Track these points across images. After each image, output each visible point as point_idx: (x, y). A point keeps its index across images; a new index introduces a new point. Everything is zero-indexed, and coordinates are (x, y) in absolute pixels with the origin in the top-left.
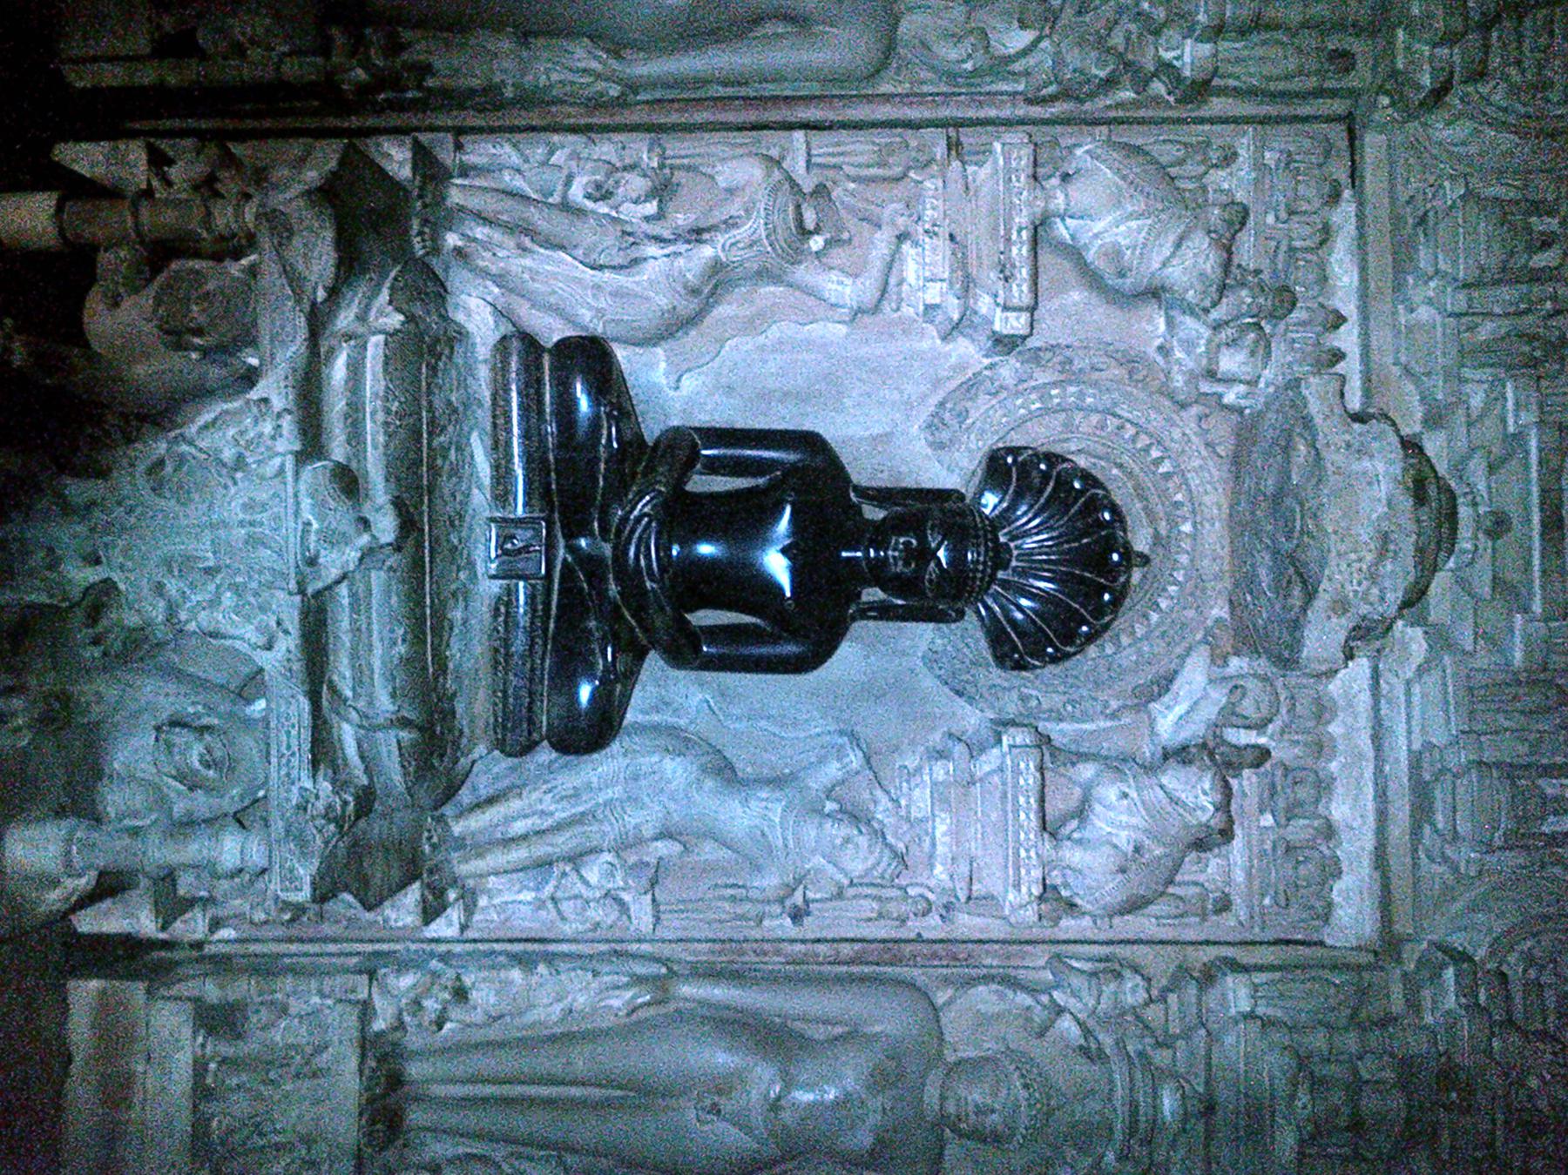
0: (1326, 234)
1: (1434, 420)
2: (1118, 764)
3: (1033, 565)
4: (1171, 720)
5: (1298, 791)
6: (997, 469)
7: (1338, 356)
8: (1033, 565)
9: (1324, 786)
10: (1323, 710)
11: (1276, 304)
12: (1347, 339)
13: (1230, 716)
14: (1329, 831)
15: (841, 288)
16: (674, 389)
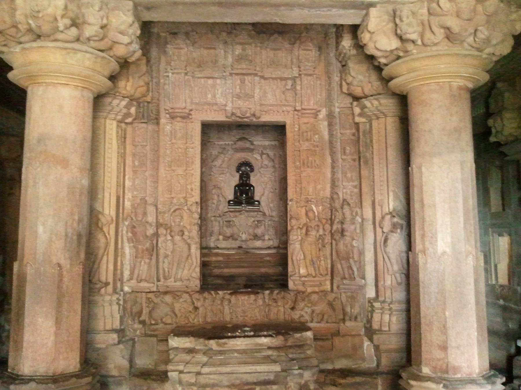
0: (218, 145)
1: (234, 136)
2: (262, 163)
3: (245, 169)
4: (259, 158)
5: (265, 147)
6: (238, 172)
8: (245, 169)
9: (265, 145)
10: (259, 145)
11: (224, 149)
13: (258, 153)
14: (268, 145)
15: (222, 184)
16: (231, 197)
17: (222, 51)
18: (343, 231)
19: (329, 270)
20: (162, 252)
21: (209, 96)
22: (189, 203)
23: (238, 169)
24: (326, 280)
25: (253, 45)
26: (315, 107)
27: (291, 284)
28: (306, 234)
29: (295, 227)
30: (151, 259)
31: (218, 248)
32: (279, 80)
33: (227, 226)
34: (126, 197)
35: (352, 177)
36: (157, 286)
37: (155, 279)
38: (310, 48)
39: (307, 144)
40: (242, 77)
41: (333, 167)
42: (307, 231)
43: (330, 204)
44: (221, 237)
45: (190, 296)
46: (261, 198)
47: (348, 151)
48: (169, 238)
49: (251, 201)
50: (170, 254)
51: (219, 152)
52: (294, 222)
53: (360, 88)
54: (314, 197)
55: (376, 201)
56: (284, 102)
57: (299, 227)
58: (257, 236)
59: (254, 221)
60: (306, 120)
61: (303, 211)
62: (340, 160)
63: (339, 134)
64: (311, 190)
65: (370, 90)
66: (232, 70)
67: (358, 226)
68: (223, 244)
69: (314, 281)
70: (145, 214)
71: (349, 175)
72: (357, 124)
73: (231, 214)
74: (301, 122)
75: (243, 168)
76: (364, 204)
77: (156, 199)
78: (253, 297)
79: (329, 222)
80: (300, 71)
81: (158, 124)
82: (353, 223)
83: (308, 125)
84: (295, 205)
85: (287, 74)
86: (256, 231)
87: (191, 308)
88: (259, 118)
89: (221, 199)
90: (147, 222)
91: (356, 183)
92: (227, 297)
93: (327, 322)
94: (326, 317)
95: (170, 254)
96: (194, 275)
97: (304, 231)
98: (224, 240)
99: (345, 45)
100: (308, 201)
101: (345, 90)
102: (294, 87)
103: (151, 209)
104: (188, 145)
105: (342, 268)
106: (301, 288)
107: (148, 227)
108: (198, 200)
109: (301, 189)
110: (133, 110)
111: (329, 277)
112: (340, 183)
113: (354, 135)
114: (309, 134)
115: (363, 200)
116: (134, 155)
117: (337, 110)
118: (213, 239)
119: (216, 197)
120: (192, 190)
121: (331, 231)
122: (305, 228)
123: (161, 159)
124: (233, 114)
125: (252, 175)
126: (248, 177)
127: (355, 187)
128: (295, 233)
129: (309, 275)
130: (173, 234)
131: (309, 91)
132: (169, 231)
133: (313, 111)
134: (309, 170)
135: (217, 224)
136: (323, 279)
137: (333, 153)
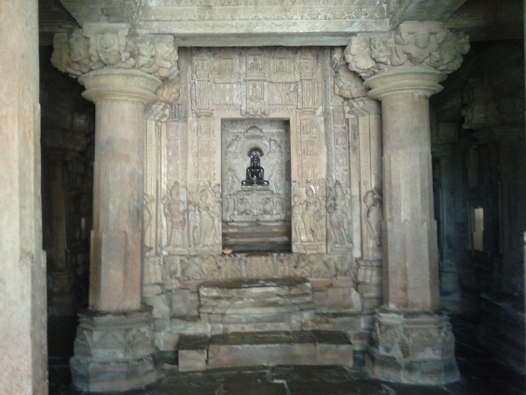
0: (232, 133)
1: (246, 125)
2: (270, 148)
3: (255, 153)
4: (267, 143)
5: (273, 134)
6: (249, 156)
7: (241, 132)
8: (255, 153)
10: (267, 133)
12: (240, 131)
13: (267, 140)
15: (236, 167)
16: (244, 177)
17: (238, 61)
18: (335, 205)
19: (325, 237)
20: (192, 224)
21: (228, 98)
22: (213, 185)
23: (250, 154)
24: (321, 244)
25: (263, 56)
26: (313, 106)
27: (294, 249)
28: (306, 208)
29: (297, 203)
30: (183, 229)
31: (233, 221)
32: (284, 84)
33: (240, 203)
34: (163, 181)
35: (343, 162)
36: (189, 250)
37: (187, 245)
38: (309, 58)
39: (307, 136)
40: (254, 82)
41: (328, 155)
42: (307, 205)
43: (326, 184)
44: (236, 213)
45: (215, 258)
46: (269, 179)
47: (339, 142)
48: (197, 212)
49: (260, 181)
50: (198, 225)
51: (232, 139)
52: (296, 199)
53: (349, 92)
54: (313, 179)
55: (362, 181)
56: (289, 103)
57: (301, 204)
58: (266, 211)
59: (264, 199)
60: (306, 117)
61: (304, 190)
62: (334, 149)
63: (333, 127)
64: (310, 173)
65: (356, 94)
66: (246, 76)
67: (347, 202)
68: (238, 218)
69: (312, 245)
70: (178, 194)
71: (341, 161)
72: (347, 120)
73: (244, 193)
74: (302, 118)
75: (254, 153)
76: (353, 184)
77: (186, 182)
78: (264, 258)
79: (325, 199)
80: (301, 77)
81: (186, 121)
82: (344, 199)
83: (308, 121)
84: (297, 186)
85: (290, 78)
86: (265, 207)
87: (215, 268)
88: (268, 115)
89: (235, 179)
90: (180, 201)
91: (346, 167)
92: (244, 258)
93: (323, 277)
94: (322, 273)
95: (198, 225)
96: (217, 242)
97: (304, 206)
98: (238, 214)
99: (336, 57)
100: (307, 182)
101: (337, 92)
102: (296, 89)
103: (182, 190)
104: (211, 138)
105: (335, 234)
106: (303, 251)
107: (181, 205)
108: (220, 182)
109: (302, 173)
110: (167, 112)
111: (324, 242)
112: (334, 168)
113: (345, 128)
114: (308, 128)
115: (352, 181)
116: (168, 147)
117: (331, 108)
118: (229, 214)
119: (230, 178)
120: (214, 174)
121: (326, 206)
122: (305, 204)
123: (189, 150)
124: (247, 113)
125: (261, 158)
126: (258, 160)
127: (346, 170)
128: (297, 208)
129: (309, 241)
130: (200, 210)
131: (308, 93)
132: (197, 207)
133: (312, 109)
134: (308, 157)
135: (232, 201)
136: (319, 243)
137: (328, 144)
